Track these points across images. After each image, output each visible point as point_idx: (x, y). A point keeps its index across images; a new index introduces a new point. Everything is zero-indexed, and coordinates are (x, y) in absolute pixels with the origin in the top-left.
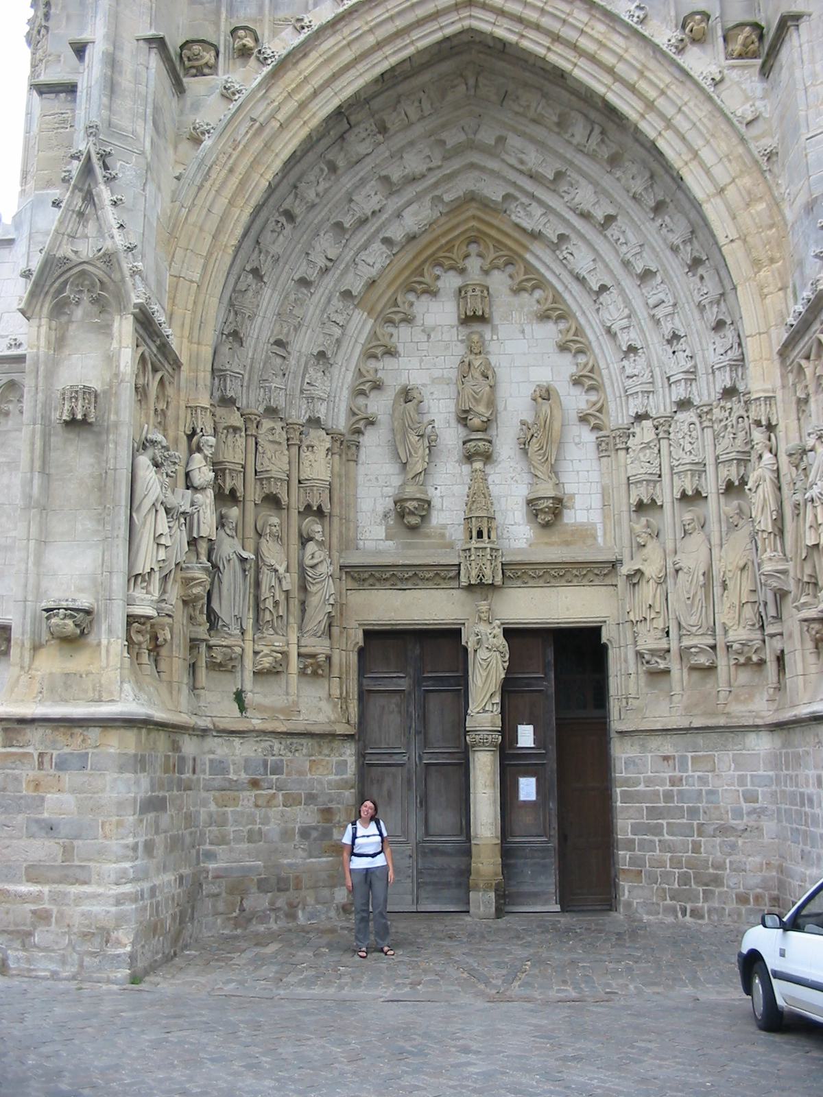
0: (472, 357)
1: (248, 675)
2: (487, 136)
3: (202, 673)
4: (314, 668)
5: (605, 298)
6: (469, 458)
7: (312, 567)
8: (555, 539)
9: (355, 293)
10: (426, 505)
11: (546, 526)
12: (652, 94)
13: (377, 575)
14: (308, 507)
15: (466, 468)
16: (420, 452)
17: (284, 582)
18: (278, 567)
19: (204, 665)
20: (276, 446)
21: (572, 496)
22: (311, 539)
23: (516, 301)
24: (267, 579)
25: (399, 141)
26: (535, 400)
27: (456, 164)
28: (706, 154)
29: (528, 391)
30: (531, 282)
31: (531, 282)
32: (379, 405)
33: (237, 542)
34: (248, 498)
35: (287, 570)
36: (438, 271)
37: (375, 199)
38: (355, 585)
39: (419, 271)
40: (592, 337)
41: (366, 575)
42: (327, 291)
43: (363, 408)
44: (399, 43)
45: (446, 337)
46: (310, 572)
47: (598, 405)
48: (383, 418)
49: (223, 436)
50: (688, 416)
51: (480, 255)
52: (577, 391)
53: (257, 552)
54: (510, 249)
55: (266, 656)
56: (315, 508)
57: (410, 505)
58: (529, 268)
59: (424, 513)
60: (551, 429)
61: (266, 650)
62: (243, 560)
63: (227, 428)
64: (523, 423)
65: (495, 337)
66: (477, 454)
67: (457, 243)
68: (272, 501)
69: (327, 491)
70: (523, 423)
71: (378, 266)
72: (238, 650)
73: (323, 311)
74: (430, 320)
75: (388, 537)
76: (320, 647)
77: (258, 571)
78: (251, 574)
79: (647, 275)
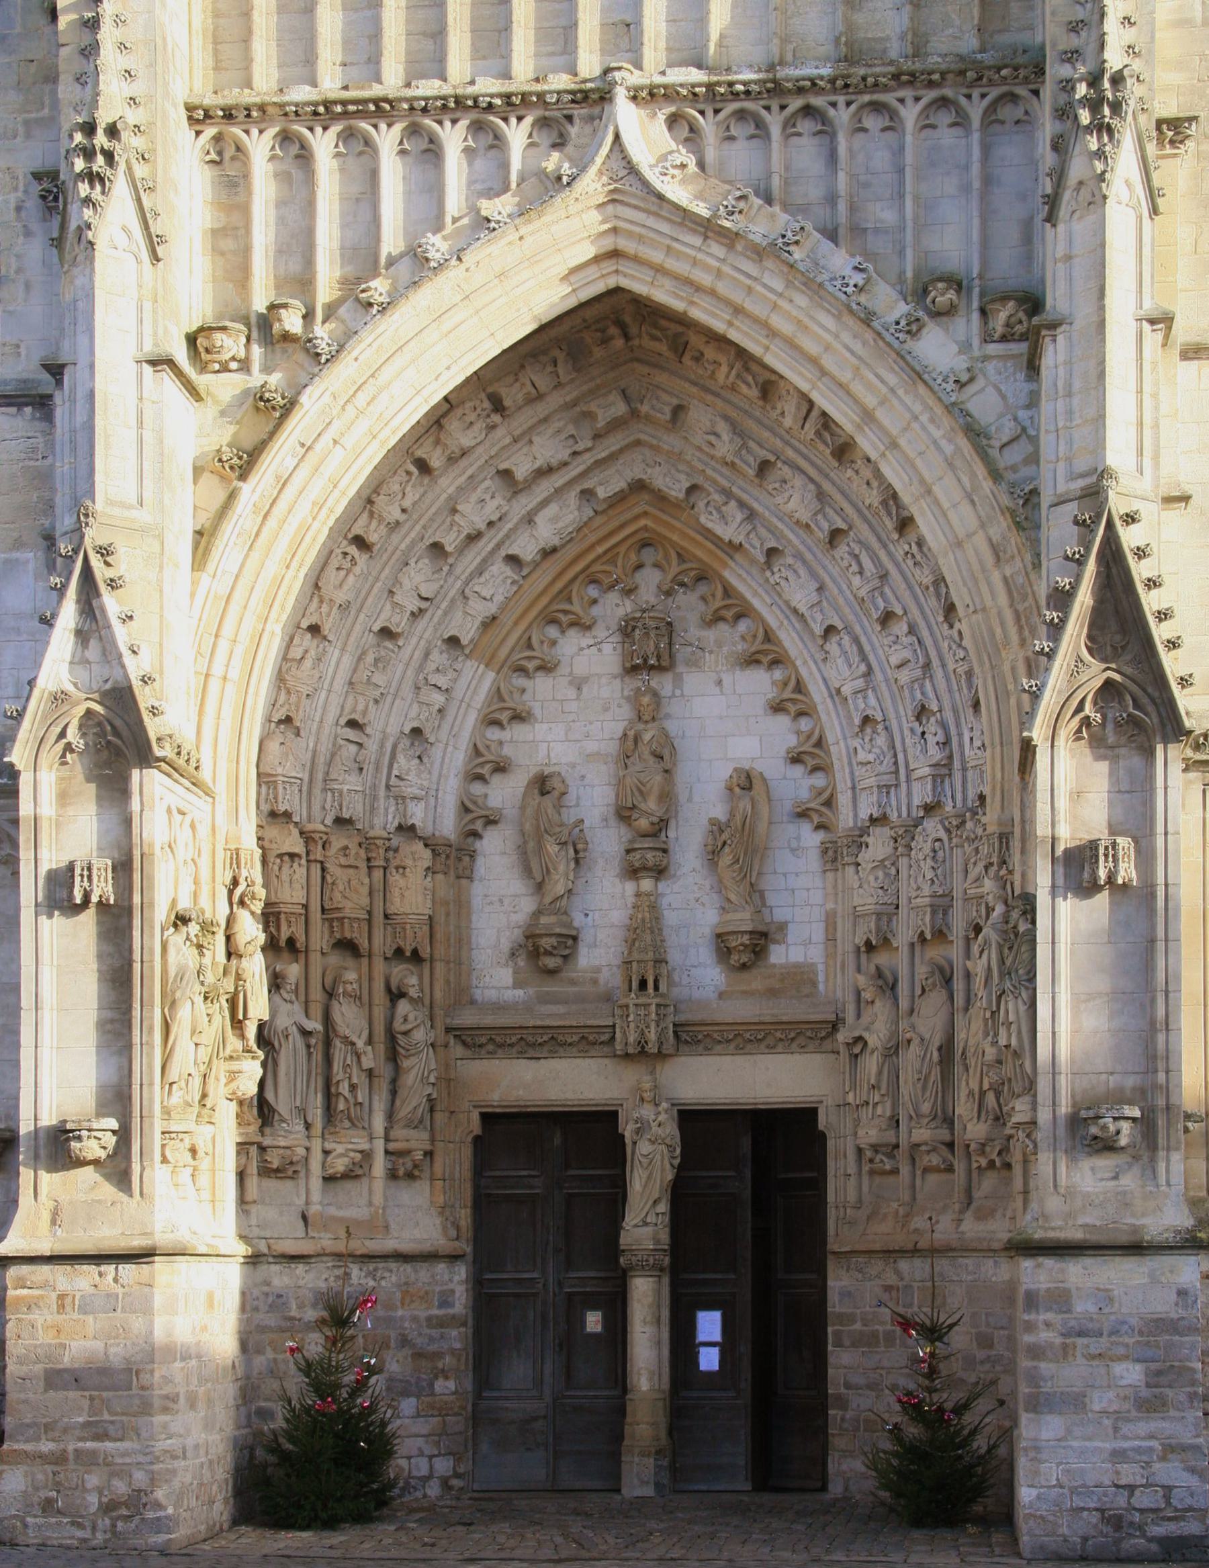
0: (641, 726)
1: (316, 1183)
3: (253, 1182)
4: (403, 1171)
5: (832, 646)
6: (633, 873)
7: (405, 1033)
9: (464, 641)
10: (570, 941)
13: (498, 1039)
14: (399, 952)
15: (630, 887)
16: (562, 868)
17: (363, 1059)
18: (354, 1039)
19: (255, 1171)
20: (351, 871)
22: (402, 995)
23: (711, 635)
24: (339, 1052)
26: (730, 789)
27: (614, 443)
32: (503, 794)
33: (298, 1008)
34: (312, 947)
35: (370, 1042)
36: (593, 591)
37: (492, 505)
38: (469, 1053)
39: (565, 594)
41: (483, 1040)
42: (423, 643)
43: (480, 801)
45: (605, 692)
46: (401, 1040)
47: (826, 795)
48: (510, 812)
49: (276, 868)
51: (656, 565)
53: (327, 1019)
54: (700, 560)
55: (341, 1155)
56: (408, 954)
57: (547, 943)
58: (728, 591)
59: (567, 952)
60: (752, 832)
61: (340, 1149)
62: (305, 1033)
63: (280, 856)
65: (678, 692)
66: (645, 868)
67: (622, 549)
68: (347, 946)
69: (426, 928)
70: (713, 822)
71: (499, 598)
72: (301, 1151)
73: (421, 668)
74: (581, 666)
75: (517, 985)
76: (417, 1140)
77: (328, 1044)
78: (318, 1056)
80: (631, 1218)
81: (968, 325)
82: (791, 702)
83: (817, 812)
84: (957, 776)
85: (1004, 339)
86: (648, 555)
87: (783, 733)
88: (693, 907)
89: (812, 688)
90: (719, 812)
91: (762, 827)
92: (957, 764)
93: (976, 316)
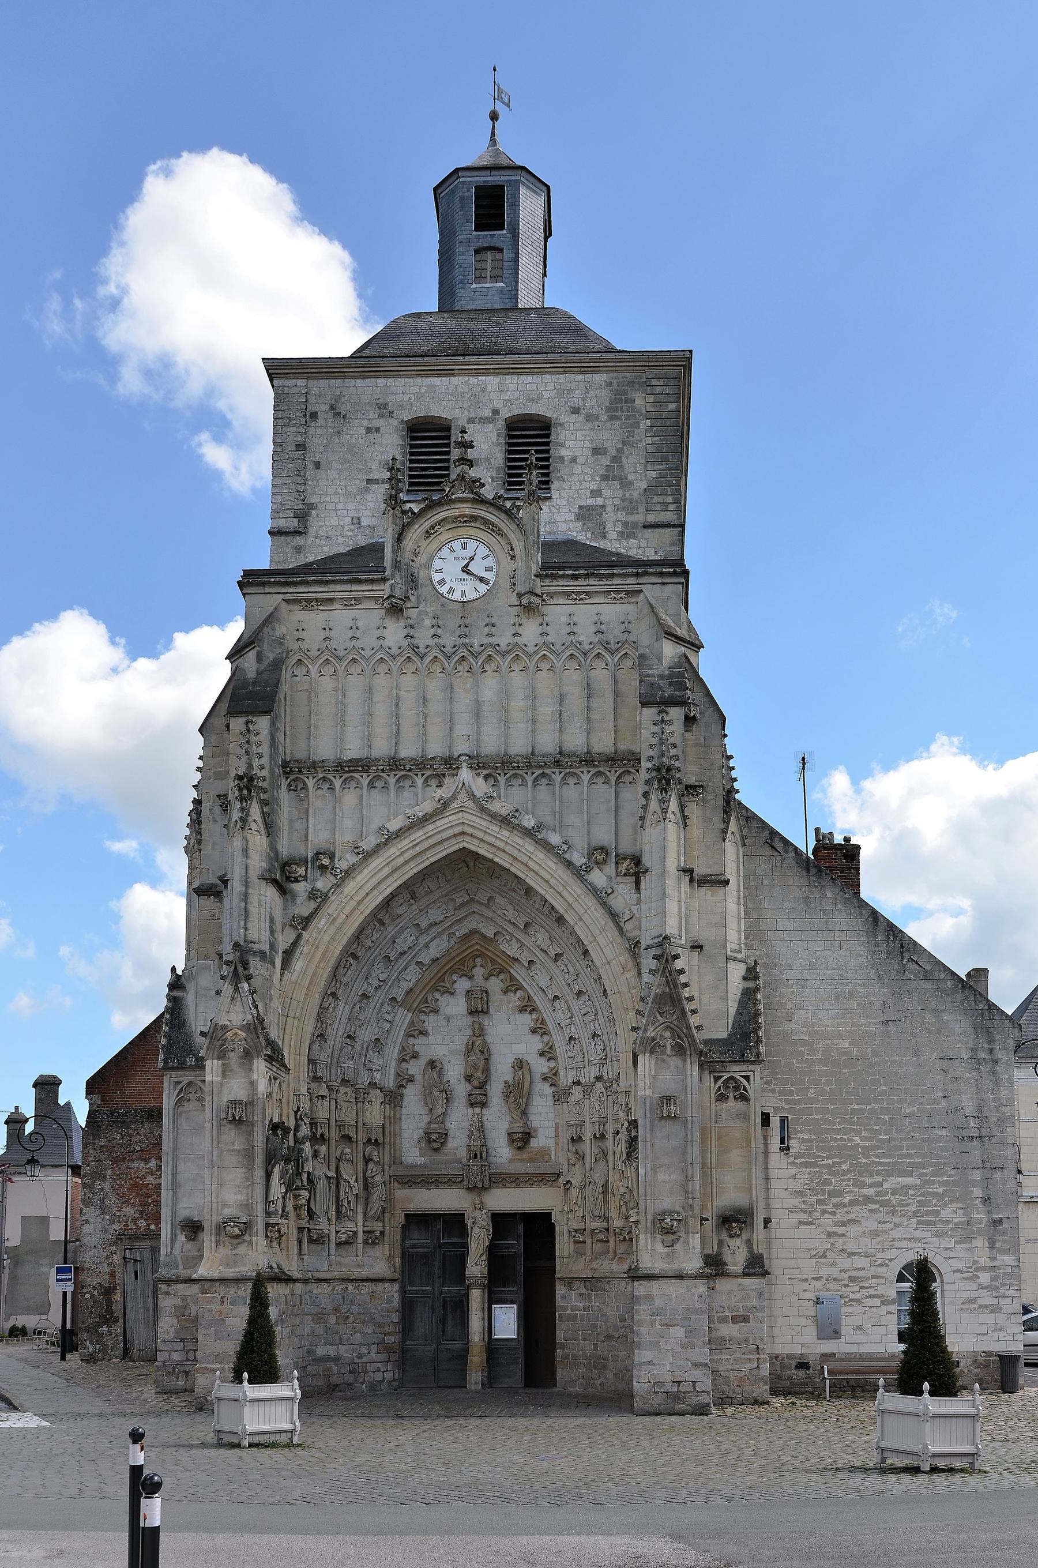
2: (482, 897)
5: (556, 1004)
8: (525, 1156)
11: (519, 1148)
12: (571, 900)
21: (536, 1130)
25: (425, 901)
28: (600, 939)
29: (510, 1060)
30: (513, 986)
31: (513, 986)
40: (551, 1028)
44: (419, 860)
50: (599, 1086)
52: (543, 1060)
64: (506, 1082)
70: (506, 1082)
79: (580, 993)
80: (470, 1262)
81: (610, 869)
82: (539, 1029)
83: (551, 1078)
84: (609, 1064)
85: (625, 875)
86: (479, 961)
87: (536, 1043)
88: (498, 1120)
89: (548, 1023)
90: (509, 1078)
91: (527, 1085)
92: (609, 1059)
93: (614, 865)
